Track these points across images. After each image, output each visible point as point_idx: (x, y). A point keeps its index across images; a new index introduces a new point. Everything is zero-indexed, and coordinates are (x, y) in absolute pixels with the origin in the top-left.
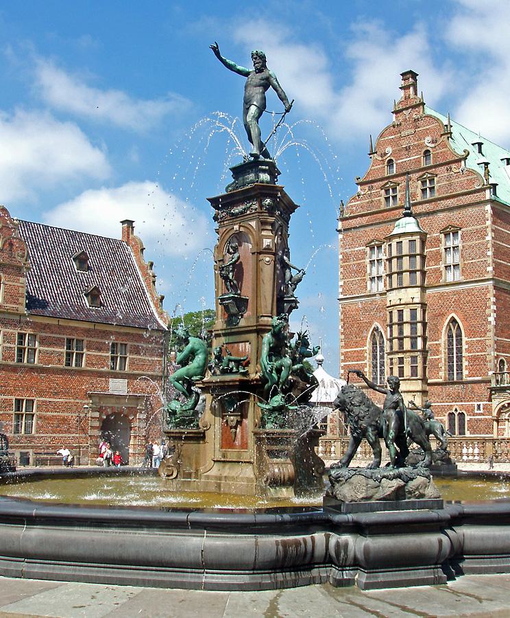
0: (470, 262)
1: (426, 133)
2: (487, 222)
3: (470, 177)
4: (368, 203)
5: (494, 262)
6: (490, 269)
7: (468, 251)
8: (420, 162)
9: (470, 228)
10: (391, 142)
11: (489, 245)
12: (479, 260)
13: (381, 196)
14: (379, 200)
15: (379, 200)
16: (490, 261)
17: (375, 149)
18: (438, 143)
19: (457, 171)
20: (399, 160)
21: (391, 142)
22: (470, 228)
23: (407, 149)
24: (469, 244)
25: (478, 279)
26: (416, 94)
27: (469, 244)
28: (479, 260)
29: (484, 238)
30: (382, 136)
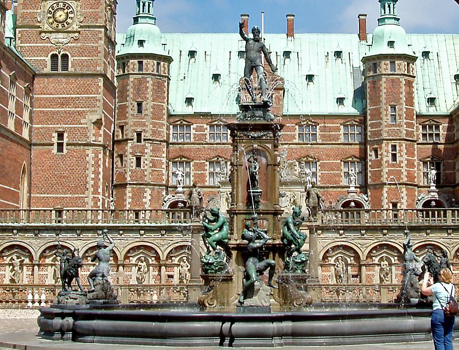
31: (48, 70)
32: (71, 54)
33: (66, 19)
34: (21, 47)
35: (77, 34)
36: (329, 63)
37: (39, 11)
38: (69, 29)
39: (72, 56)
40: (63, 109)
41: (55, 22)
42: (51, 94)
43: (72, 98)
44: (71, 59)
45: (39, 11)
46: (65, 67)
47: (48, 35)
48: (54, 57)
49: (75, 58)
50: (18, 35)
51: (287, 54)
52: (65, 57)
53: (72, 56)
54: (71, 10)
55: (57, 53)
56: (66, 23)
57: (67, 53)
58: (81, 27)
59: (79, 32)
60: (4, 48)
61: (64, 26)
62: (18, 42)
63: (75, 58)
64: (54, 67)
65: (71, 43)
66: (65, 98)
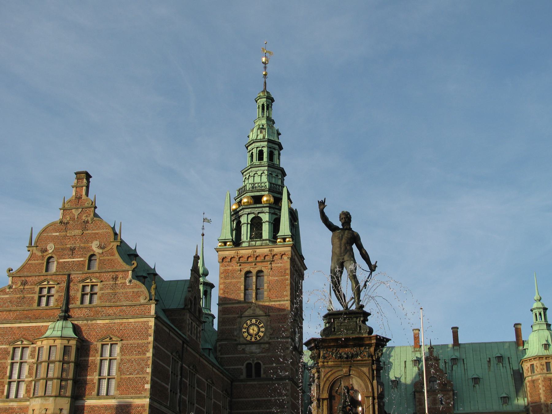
0: (128, 376)
1: (95, 237)
2: (149, 338)
3: (136, 290)
4: (19, 298)
5: (152, 379)
6: (148, 386)
7: (128, 365)
8: (84, 265)
9: (131, 342)
10: (53, 239)
11: (150, 362)
12: (138, 376)
13: (35, 293)
14: (33, 298)
15: (33, 298)
16: (149, 378)
17: (36, 242)
18: (106, 249)
19: (123, 281)
20: (61, 259)
21: (53, 239)
22: (131, 342)
23: (72, 250)
24: (128, 357)
25: (133, 395)
26: (87, 194)
27: (128, 357)
28: (138, 376)
29: (145, 354)
30: (44, 230)
31: (244, 376)
32: (263, 362)
33: (258, 333)
34: (221, 358)
35: (267, 346)
36: (492, 368)
37: (235, 327)
38: (261, 341)
39: (264, 364)
40: (257, 411)
41: (249, 336)
42: (247, 398)
43: (265, 401)
44: (263, 367)
45: (235, 327)
46: (258, 373)
47: (243, 346)
48: (249, 366)
49: (266, 366)
50: (219, 348)
51: (454, 361)
52: (258, 365)
53: (264, 364)
54: (262, 325)
55: (251, 362)
56: (258, 336)
57: (260, 361)
58: (270, 338)
59: (269, 343)
60: (200, 356)
61: (257, 339)
62: (219, 354)
63: (266, 366)
64: (249, 375)
65: (263, 353)
66: (259, 401)
